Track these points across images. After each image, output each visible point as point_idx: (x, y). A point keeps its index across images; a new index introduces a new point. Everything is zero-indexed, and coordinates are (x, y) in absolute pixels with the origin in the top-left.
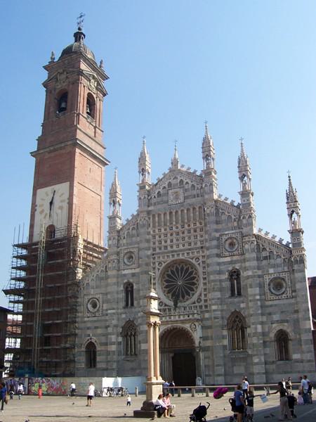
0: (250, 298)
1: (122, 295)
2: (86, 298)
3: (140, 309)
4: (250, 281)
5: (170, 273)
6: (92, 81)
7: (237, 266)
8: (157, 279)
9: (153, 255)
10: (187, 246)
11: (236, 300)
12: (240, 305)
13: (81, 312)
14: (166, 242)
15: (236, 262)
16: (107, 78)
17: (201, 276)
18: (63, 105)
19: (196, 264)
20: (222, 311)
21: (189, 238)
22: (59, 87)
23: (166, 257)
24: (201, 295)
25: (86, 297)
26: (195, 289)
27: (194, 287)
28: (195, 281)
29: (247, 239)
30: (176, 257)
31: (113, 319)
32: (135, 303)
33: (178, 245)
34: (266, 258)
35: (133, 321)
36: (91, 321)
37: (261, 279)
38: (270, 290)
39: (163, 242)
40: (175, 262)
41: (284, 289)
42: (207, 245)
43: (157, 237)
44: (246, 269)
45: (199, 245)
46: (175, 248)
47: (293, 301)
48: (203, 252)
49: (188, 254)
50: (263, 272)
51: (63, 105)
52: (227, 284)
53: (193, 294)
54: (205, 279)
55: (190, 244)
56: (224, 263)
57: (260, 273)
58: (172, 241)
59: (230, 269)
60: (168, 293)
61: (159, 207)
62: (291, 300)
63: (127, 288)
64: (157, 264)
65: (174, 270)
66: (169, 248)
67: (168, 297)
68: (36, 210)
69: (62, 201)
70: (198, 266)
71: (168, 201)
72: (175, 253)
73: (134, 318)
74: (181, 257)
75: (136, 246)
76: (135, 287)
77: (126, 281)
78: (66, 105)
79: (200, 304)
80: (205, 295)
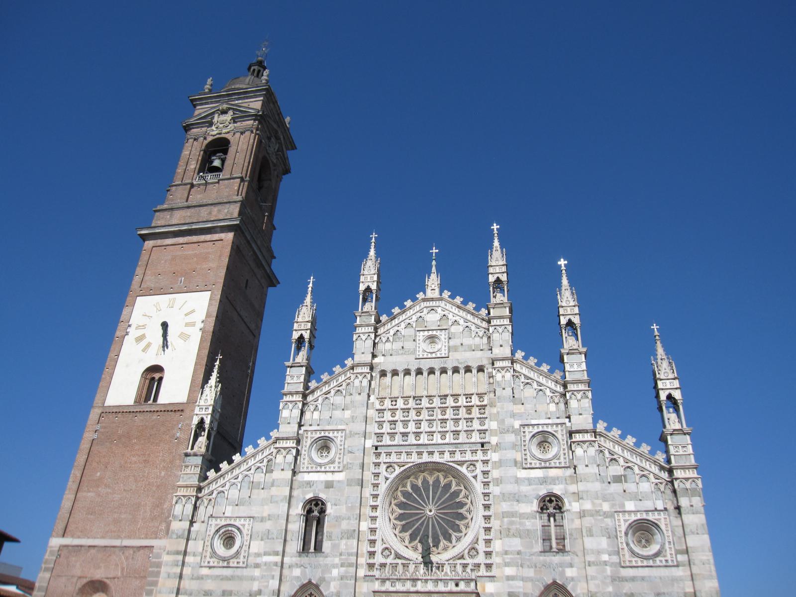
0: (590, 558)
1: (297, 526)
2: (214, 524)
3: (337, 560)
4: (588, 521)
5: (409, 488)
6: (273, 140)
7: (557, 490)
8: (380, 498)
9: (376, 449)
10: (449, 438)
11: (557, 559)
12: (563, 572)
13: (194, 555)
14: (405, 423)
15: (554, 480)
16: (294, 148)
17: (480, 501)
18: (217, 163)
19: (469, 475)
20: (523, 579)
21: (456, 421)
22: (213, 132)
23: (404, 456)
24: (477, 543)
25: (213, 522)
26: (463, 528)
27: (461, 524)
28: (463, 511)
29: (578, 437)
30: (425, 458)
31: (273, 577)
32: (326, 545)
33: (431, 433)
34: (618, 479)
35: (317, 587)
36: (217, 577)
37: (608, 521)
38: (628, 544)
39: (400, 428)
40: (421, 468)
41: (654, 548)
42: (494, 440)
43: (388, 416)
44: (578, 496)
45: (476, 438)
46: (424, 439)
47: (680, 572)
48: (485, 452)
49: (452, 453)
50: (613, 505)
51: (217, 163)
52: (536, 524)
53: (458, 539)
54: (487, 507)
55: (456, 433)
56: (530, 481)
57: (606, 507)
58: (418, 423)
59: (543, 492)
60: (404, 529)
61: (394, 359)
62: (674, 569)
63: (310, 511)
64: (383, 467)
65: (420, 483)
66: (412, 439)
67: (403, 540)
68: (127, 334)
69: (187, 325)
70: (473, 480)
71: (415, 350)
72: (425, 451)
73: (323, 579)
74: (436, 458)
75: (340, 427)
76: (329, 510)
77: (309, 496)
78: (223, 164)
79: (476, 561)
80: (488, 542)
